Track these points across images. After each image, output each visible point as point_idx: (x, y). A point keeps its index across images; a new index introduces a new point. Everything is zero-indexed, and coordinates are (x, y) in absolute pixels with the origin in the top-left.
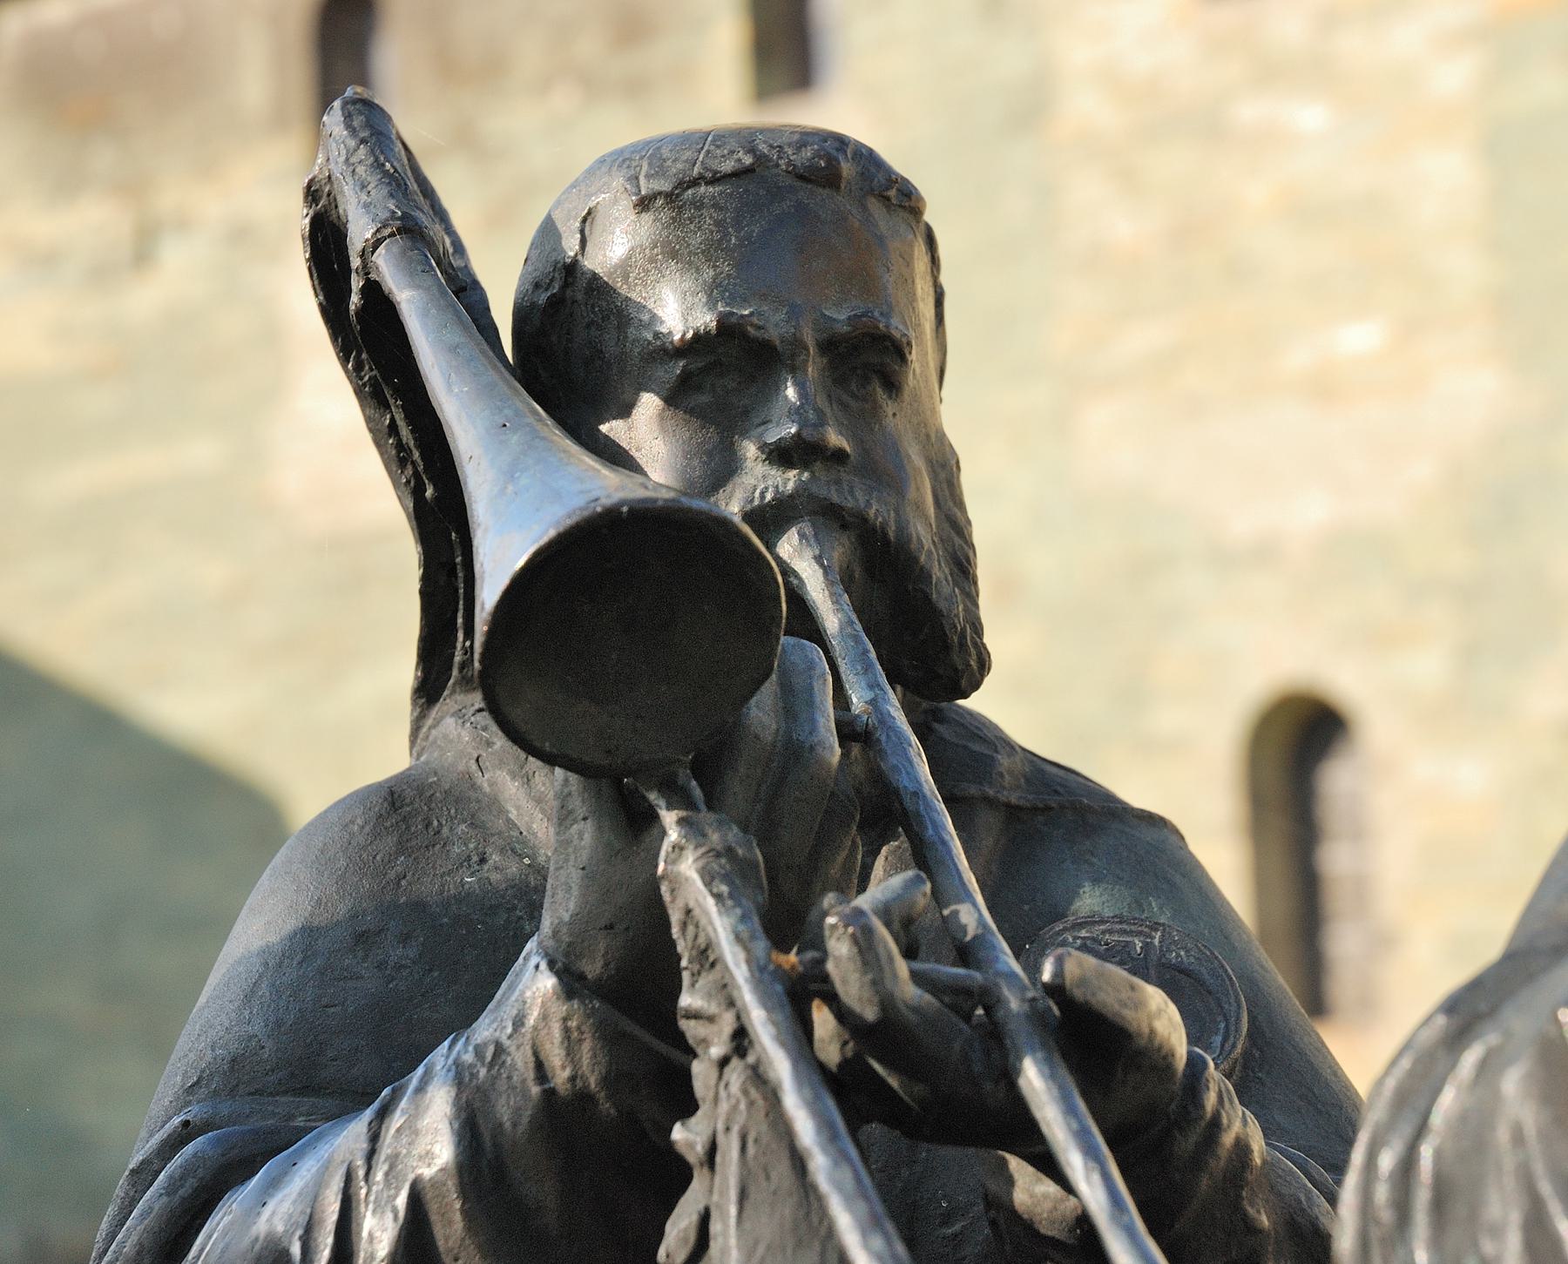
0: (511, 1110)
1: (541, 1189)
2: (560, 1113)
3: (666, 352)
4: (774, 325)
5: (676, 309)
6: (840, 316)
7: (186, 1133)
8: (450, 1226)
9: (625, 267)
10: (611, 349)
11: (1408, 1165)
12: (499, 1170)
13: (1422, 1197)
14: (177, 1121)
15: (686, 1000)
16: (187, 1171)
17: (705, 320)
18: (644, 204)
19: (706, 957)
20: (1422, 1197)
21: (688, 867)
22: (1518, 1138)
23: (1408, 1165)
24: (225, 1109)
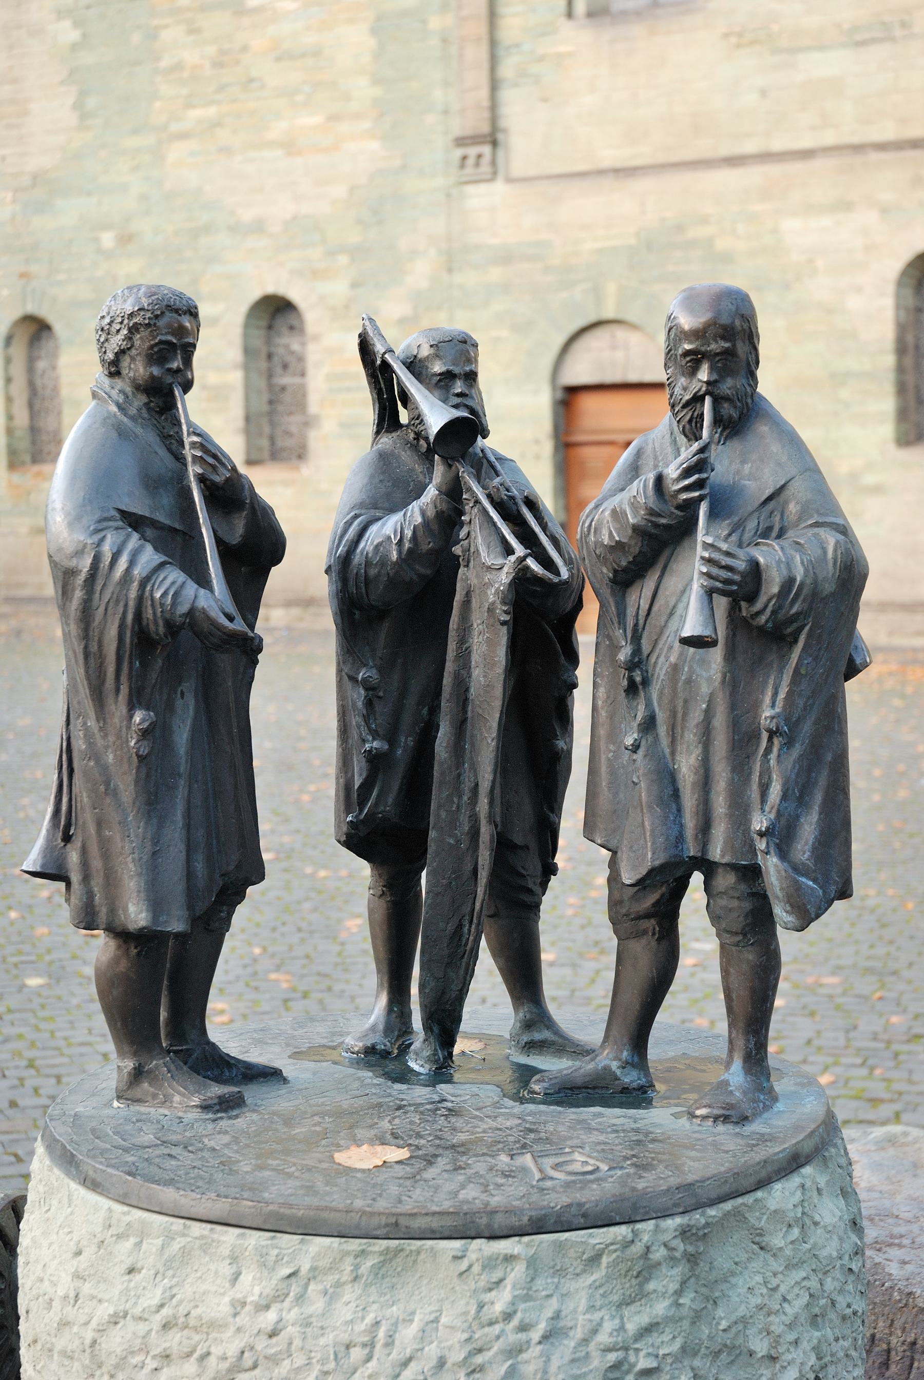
0: (431, 513)
1: (435, 527)
2: (439, 515)
3: (436, 375)
4: (456, 370)
5: (438, 368)
6: (467, 369)
7: (356, 517)
8: (420, 533)
9: (428, 357)
10: (424, 373)
11: (590, 525)
12: (428, 525)
13: (592, 531)
14: (352, 514)
15: (464, 497)
16: (361, 522)
17: (444, 369)
18: (431, 346)
19: (470, 489)
20: (592, 531)
21: (465, 475)
22: (608, 522)
23: (590, 525)
24: (363, 511)
